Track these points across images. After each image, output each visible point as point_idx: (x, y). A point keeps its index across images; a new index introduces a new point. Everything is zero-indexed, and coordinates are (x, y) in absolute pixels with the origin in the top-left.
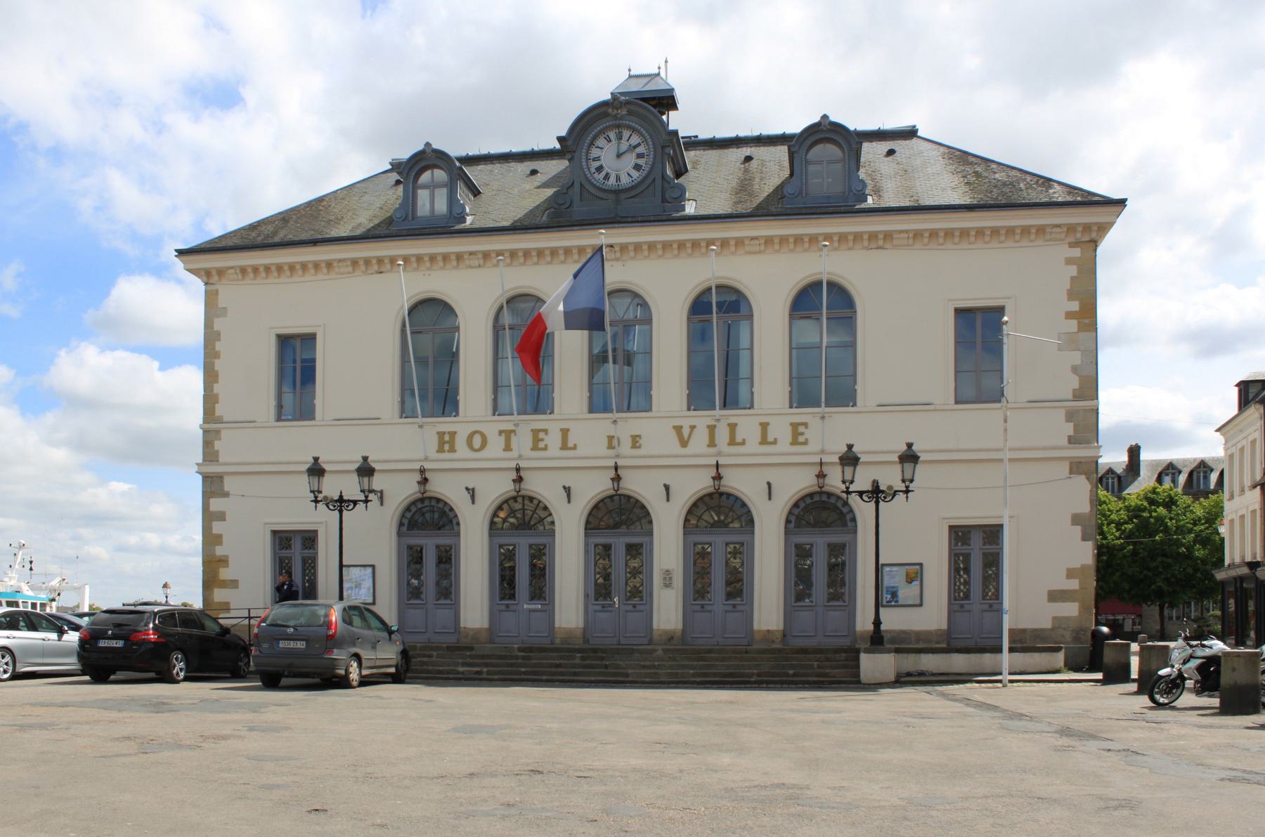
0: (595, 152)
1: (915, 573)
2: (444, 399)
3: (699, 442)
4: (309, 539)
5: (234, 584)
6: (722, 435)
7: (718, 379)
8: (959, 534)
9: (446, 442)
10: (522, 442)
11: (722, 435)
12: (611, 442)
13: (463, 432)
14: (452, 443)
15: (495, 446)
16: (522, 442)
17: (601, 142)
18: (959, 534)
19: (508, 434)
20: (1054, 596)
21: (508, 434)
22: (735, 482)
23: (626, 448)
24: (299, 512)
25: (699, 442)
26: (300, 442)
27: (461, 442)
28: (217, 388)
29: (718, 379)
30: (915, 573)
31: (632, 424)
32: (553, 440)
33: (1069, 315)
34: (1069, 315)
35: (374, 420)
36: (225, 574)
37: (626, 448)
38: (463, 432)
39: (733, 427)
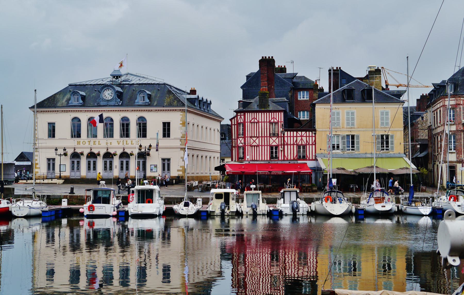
0: (104, 93)
1: (156, 166)
2: (79, 136)
3: (121, 144)
4: (54, 160)
5: (39, 168)
6: (125, 143)
7: (125, 132)
8: (163, 160)
9: (79, 143)
10: (92, 143)
11: (125, 143)
12: (107, 143)
13: (82, 141)
14: (79, 143)
15: (87, 144)
16: (92, 143)
17: (105, 91)
18: (163, 160)
19: (89, 142)
20: (178, 171)
21: (89, 142)
22: (127, 150)
23: (109, 145)
24: (52, 155)
25: (121, 144)
26: (53, 143)
27: (81, 143)
28: (36, 132)
29: (125, 132)
30: (156, 166)
31: (110, 140)
32: (97, 143)
33: (181, 124)
34: (181, 124)
35: (66, 139)
36: (37, 166)
37: (109, 145)
38: (82, 141)
39: (127, 141)
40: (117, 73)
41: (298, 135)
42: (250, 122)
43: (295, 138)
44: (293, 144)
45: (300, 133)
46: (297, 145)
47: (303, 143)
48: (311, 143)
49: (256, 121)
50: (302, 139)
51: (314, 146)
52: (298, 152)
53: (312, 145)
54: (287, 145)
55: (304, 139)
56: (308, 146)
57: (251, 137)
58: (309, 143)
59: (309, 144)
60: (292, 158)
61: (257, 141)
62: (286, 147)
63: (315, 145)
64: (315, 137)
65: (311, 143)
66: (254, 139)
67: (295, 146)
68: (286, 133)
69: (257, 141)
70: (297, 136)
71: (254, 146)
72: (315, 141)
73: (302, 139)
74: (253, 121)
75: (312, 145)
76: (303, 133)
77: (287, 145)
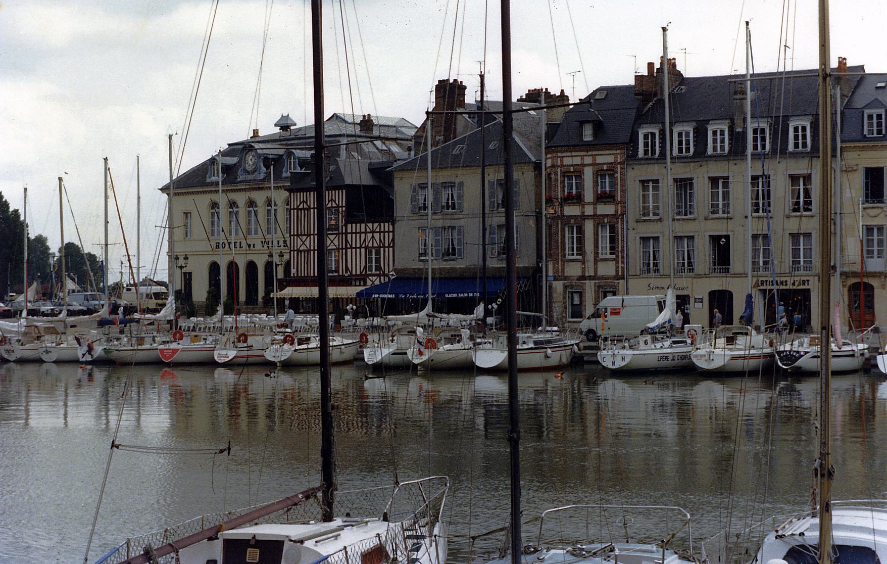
40: (283, 122)
41: (368, 230)
42: (298, 209)
43: (363, 235)
44: (361, 247)
45: (370, 225)
46: (366, 248)
47: (375, 245)
48: (387, 245)
49: (305, 206)
50: (373, 237)
51: (391, 249)
52: (368, 260)
53: (389, 247)
54: (351, 248)
55: (377, 235)
56: (382, 250)
57: (298, 235)
58: (384, 244)
59: (384, 247)
60: (358, 273)
61: (307, 243)
62: (349, 251)
63: (393, 247)
64: (393, 232)
65: (387, 245)
66: (304, 238)
67: (363, 250)
68: (349, 226)
69: (307, 243)
70: (366, 233)
71: (304, 251)
72: (393, 240)
73: (373, 237)
74: (301, 206)
75: (389, 247)
76: (376, 225)
77: (351, 248)
